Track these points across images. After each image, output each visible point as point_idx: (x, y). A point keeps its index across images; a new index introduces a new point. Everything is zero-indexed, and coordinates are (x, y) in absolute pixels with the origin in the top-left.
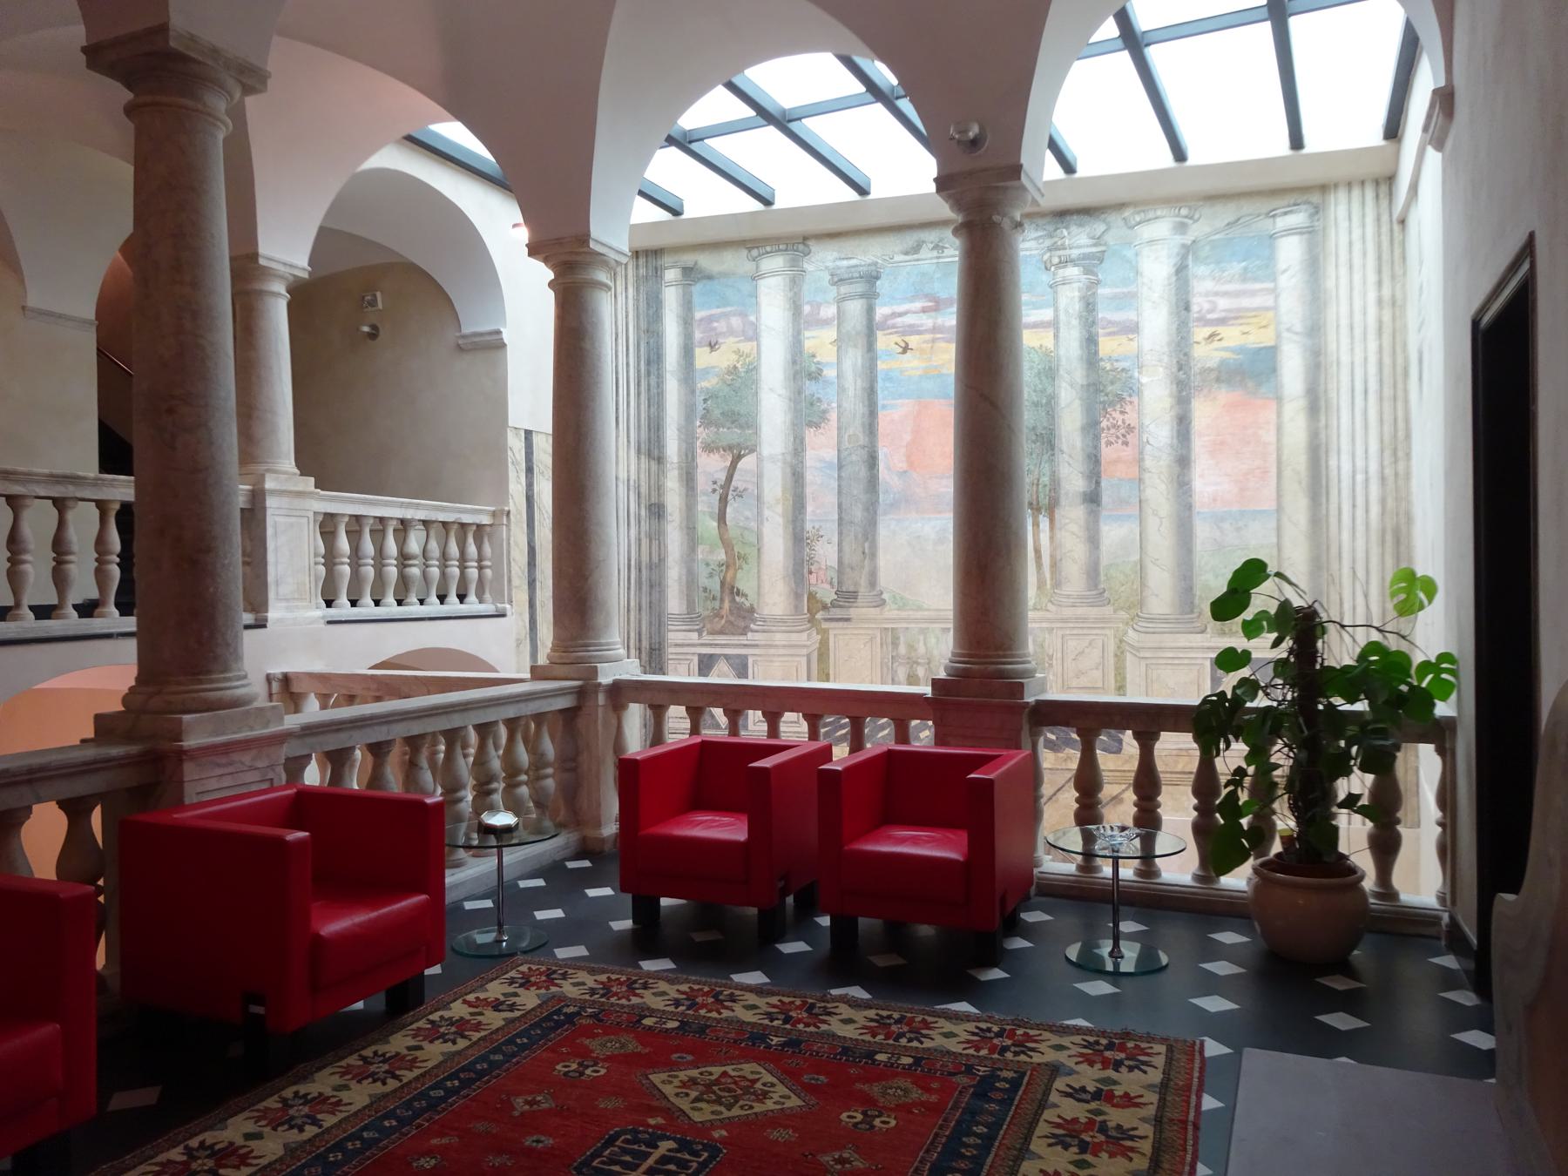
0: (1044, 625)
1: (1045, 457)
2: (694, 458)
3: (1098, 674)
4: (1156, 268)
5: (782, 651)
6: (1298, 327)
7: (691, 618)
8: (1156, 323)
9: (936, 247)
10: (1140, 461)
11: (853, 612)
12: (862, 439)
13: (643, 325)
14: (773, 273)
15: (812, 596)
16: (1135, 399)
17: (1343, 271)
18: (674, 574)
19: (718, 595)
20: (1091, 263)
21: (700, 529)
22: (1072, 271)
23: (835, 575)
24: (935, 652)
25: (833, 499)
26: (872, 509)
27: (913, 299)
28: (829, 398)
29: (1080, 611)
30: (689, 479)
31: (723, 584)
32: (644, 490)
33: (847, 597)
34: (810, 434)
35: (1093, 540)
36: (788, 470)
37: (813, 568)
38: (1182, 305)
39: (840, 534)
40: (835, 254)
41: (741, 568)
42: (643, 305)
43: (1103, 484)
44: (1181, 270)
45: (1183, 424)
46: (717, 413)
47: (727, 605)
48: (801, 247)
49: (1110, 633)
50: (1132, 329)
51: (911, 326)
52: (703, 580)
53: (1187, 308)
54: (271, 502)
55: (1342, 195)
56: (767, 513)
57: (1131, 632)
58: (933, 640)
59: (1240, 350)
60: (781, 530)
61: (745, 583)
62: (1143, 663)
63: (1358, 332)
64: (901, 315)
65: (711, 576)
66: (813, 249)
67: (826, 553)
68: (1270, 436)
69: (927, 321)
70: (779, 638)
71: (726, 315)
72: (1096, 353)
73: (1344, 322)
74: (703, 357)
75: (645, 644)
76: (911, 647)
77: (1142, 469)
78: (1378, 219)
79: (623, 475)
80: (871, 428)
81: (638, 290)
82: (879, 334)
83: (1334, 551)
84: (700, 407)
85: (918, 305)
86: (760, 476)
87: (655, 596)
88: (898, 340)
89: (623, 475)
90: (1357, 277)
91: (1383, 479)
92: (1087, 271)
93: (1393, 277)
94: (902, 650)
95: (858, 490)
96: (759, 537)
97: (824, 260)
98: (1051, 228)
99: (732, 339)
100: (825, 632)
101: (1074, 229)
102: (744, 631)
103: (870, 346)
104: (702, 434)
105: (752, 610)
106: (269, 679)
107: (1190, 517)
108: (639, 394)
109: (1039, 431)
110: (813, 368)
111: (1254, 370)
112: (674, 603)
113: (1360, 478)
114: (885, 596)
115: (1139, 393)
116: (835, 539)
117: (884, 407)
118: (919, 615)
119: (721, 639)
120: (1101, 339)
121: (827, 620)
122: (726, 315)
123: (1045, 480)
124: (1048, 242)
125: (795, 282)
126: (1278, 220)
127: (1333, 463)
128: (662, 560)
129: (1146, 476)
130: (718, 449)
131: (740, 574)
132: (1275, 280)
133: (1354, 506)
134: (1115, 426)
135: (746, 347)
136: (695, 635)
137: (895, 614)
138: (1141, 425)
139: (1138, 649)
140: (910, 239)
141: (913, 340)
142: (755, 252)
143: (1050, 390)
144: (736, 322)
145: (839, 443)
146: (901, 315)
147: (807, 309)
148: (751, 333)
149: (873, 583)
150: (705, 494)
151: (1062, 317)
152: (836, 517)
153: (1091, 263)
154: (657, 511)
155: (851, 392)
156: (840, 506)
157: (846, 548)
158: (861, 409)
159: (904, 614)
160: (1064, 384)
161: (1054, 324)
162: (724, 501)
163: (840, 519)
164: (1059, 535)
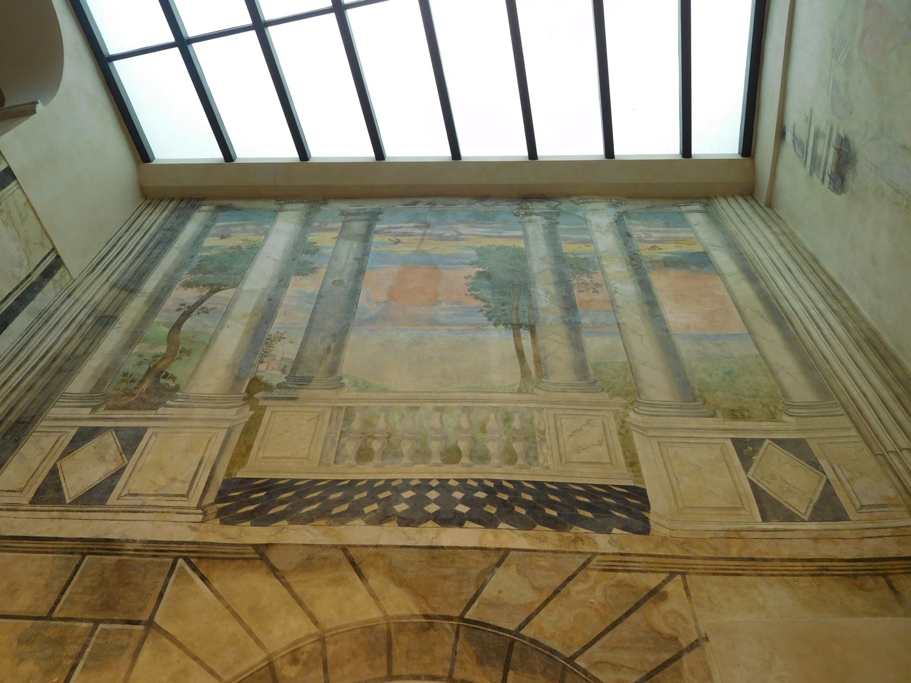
3: (602, 450)
11: (302, 393)
29: (571, 396)
57: (632, 414)
58: (397, 417)
60: (240, 334)
62: (654, 442)
65: (140, 364)
76: (367, 423)
83: (817, 355)
90: (751, 226)
94: (356, 425)
102: (155, 407)
107: (669, 336)
114: (345, 381)
117: (371, 268)
118: (382, 396)
127: (785, 304)
133: (819, 328)
137: (354, 394)
139: (645, 429)
164: (540, 342)
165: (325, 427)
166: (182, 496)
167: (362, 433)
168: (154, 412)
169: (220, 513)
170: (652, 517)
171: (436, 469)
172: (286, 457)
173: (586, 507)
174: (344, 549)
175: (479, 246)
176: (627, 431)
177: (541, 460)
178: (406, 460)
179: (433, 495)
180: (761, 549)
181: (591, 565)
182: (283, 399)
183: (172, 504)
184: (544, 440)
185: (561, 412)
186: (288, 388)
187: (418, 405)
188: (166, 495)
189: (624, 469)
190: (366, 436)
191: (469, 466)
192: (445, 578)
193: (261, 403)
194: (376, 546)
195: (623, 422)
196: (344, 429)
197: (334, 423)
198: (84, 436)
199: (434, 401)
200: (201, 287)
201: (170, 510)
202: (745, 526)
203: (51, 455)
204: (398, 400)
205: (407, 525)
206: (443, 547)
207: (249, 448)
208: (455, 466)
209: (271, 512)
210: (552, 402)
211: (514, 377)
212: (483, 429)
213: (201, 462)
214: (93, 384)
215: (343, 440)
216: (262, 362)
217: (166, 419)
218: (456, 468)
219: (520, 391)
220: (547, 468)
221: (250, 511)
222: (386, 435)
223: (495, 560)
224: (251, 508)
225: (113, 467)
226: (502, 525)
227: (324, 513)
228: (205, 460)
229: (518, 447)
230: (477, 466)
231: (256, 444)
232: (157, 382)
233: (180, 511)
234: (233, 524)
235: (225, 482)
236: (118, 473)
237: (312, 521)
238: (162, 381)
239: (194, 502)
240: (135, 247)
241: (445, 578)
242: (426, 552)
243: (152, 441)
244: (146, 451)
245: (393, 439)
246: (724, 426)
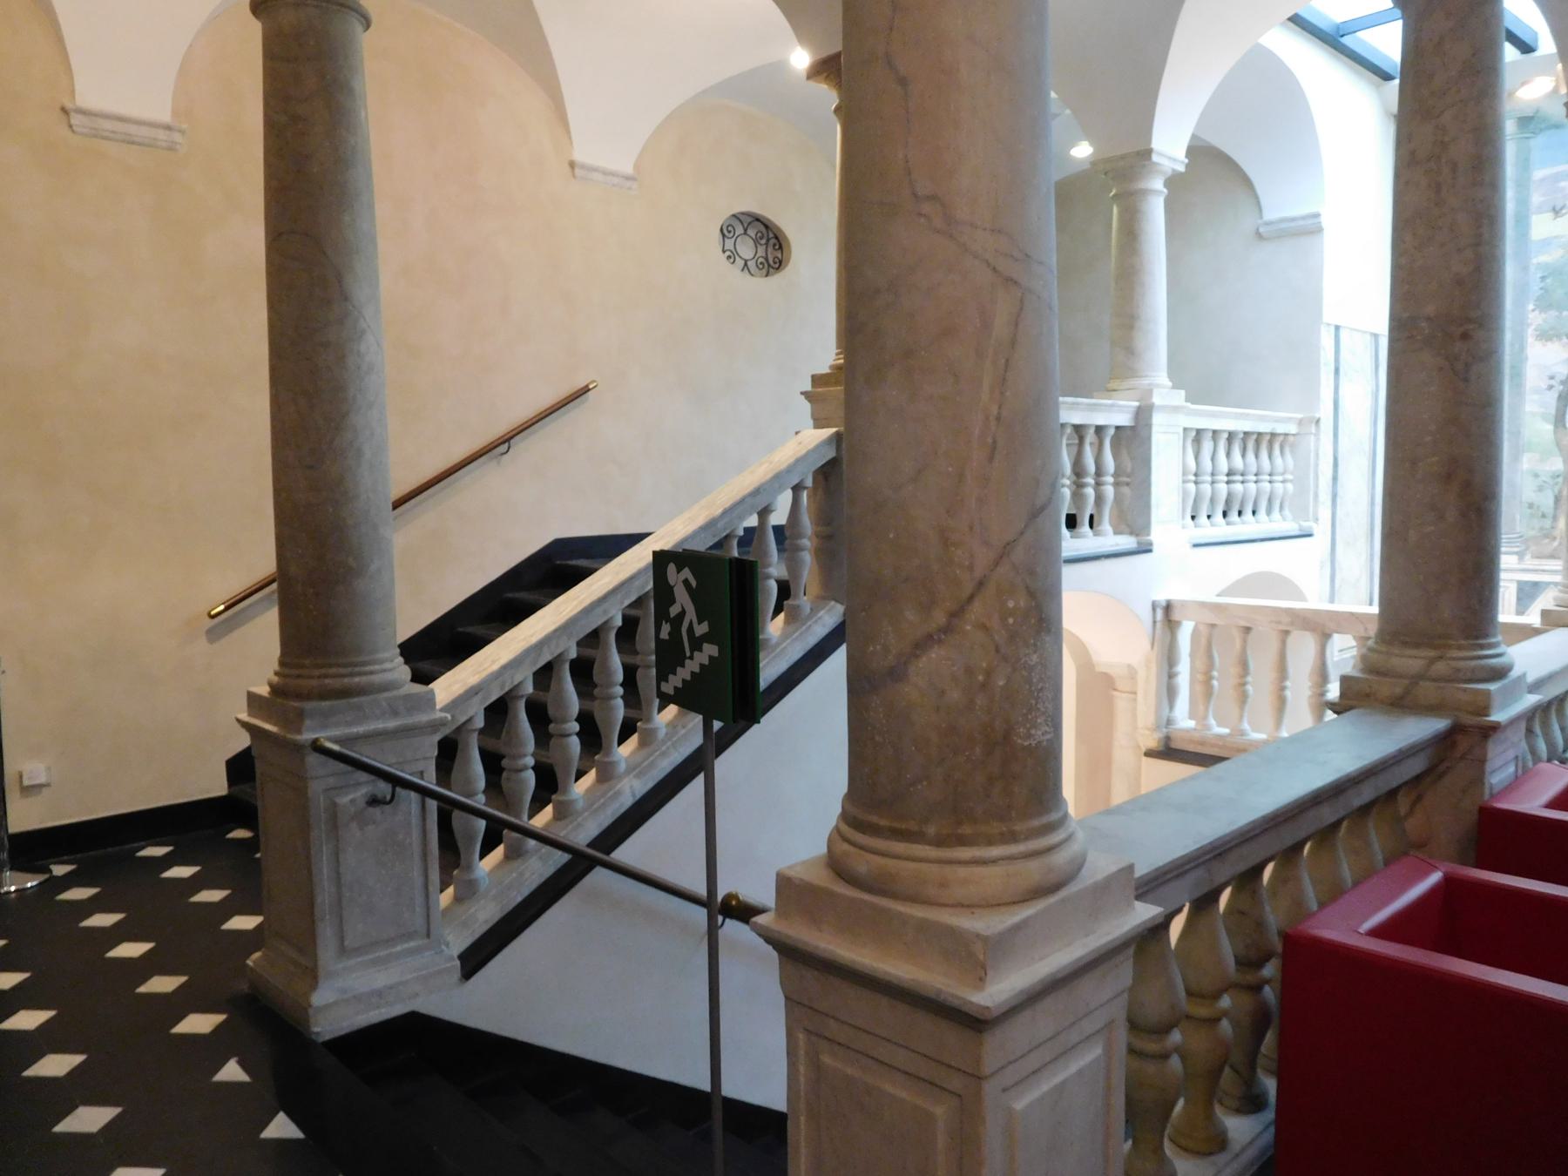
54: (1158, 420)
65: (1540, 489)
106: (1154, 606)
130: (1559, 337)
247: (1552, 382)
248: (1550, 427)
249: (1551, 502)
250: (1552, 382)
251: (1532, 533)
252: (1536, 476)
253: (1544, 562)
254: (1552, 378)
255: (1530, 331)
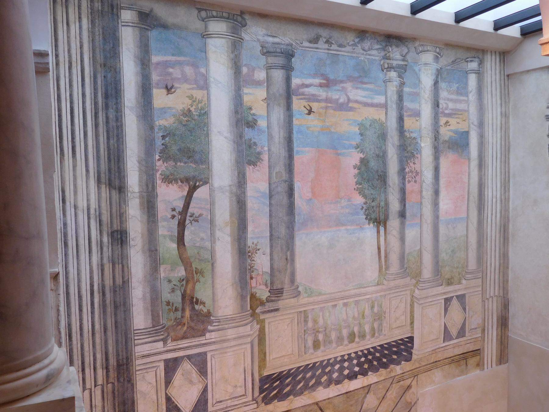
0: (382, 293)
1: (382, 190)
2: (154, 188)
3: (403, 317)
4: (427, 80)
5: (233, 343)
6: (476, 123)
7: (157, 330)
8: (426, 111)
9: (327, 42)
10: (421, 192)
11: (281, 304)
12: (285, 176)
13: (100, 58)
14: (219, 35)
15: (253, 296)
16: (419, 156)
17: (490, 96)
18: (138, 293)
19: (180, 306)
20: (402, 70)
21: (161, 250)
22: (393, 74)
23: (268, 278)
24: (329, 322)
25: (265, 221)
26: (291, 227)
27: (315, 76)
28: (262, 142)
30: (150, 206)
31: (183, 296)
32: (105, 218)
33: (277, 293)
34: (249, 170)
35: (402, 239)
36: (234, 199)
37: (254, 274)
38: (436, 105)
39: (271, 246)
40: (264, 31)
41: (198, 281)
42: (99, 39)
43: (407, 206)
44: (436, 83)
45: (437, 169)
46: (175, 148)
47: (188, 313)
48: (239, 19)
49: (408, 292)
50: (417, 114)
51: (313, 95)
52: (166, 295)
53: (438, 106)
55: (489, 56)
56: (218, 234)
57: (416, 291)
58: (328, 314)
59: (456, 132)
60: (229, 247)
61: (202, 292)
63: (494, 127)
64: (307, 86)
65: (173, 291)
66: (248, 22)
67: (262, 262)
68: (466, 180)
69: (322, 93)
70: (231, 333)
71: (180, 63)
72: (403, 127)
73: (490, 122)
74: (160, 98)
75: (113, 361)
76: (315, 322)
77: (422, 197)
78: (500, 73)
79: (82, 204)
80: (290, 168)
81: (93, 22)
82: (294, 98)
84: (159, 142)
85: (317, 81)
86: (212, 203)
87: (120, 315)
88: (306, 104)
89: (82, 204)
90: (494, 100)
91: (501, 201)
92: (400, 76)
93: (505, 102)
94: (310, 324)
95: (282, 213)
96: (213, 253)
97: (256, 33)
98: (384, 44)
99: (186, 86)
100: (263, 321)
101: (395, 49)
103: (289, 107)
104: (161, 167)
105: (209, 314)
108: (96, 125)
109: (380, 173)
110: (250, 119)
111: (459, 143)
112: (140, 319)
113: (494, 200)
115: (420, 153)
116: (268, 251)
117: (298, 152)
119: (184, 343)
120: (405, 118)
121: (264, 312)
122: (180, 63)
123: (382, 204)
124: (383, 53)
125: (236, 45)
126: (469, 64)
127: (486, 193)
128: (126, 282)
129: (423, 200)
130: (176, 180)
131: (198, 286)
132: (468, 96)
134: (411, 171)
135: (199, 94)
136: (161, 343)
138: (421, 171)
140: (313, 31)
141: (315, 106)
142: (203, 14)
143: (383, 148)
144: (189, 70)
145: (270, 178)
146: (307, 86)
147: (245, 70)
148: (202, 83)
149: (292, 281)
150: (165, 220)
151: (389, 102)
152: (268, 234)
153: (402, 70)
154: (120, 237)
155: (277, 140)
156: (271, 225)
157: (276, 257)
158: (283, 153)
159: (311, 300)
160: (390, 145)
161: (385, 106)
162: (182, 226)
163: (271, 235)
165: (296, 328)
166: (243, 395)
167: (314, 330)
168: (203, 338)
169: (264, 399)
170: (414, 351)
171: (346, 348)
172: (283, 356)
173: (396, 353)
174: (317, 404)
175: (360, 119)
176: (413, 303)
177: (383, 331)
178: (334, 345)
179: (346, 364)
180: (440, 356)
181: (394, 382)
182: (272, 311)
183: (241, 402)
184: (385, 317)
185: (392, 296)
186: (272, 301)
187: (335, 303)
188: (236, 398)
189: (409, 327)
190: (316, 332)
191: (358, 343)
192: (352, 406)
193: (262, 317)
194: (328, 399)
195: (413, 296)
196: (305, 329)
197: (300, 325)
198: (171, 367)
199: (343, 298)
200: (180, 183)
201: (241, 405)
202: (437, 347)
203: (159, 387)
204: (327, 301)
205: (338, 384)
206: (350, 391)
207: (265, 354)
208: (353, 344)
209: (284, 392)
210: (390, 289)
211: (376, 274)
212: (363, 316)
213: (245, 371)
214: (150, 317)
215: (306, 336)
216: (252, 278)
217: (214, 343)
218: (354, 345)
219: (378, 284)
220: (385, 335)
221: (276, 394)
222: (324, 329)
223: (367, 391)
224: (275, 392)
225: (200, 387)
226: (370, 373)
227: (306, 387)
228: (246, 369)
229: (376, 325)
230: (361, 342)
231: (267, 351)
232: (193, 308)
233: (245, 404)
234: (270, 403)
235: (261, 380)
236: (205, 390)
237: (303, 393)
238: (197, 307)
239: (250, 398)
240: (84, 103)
241: (352, 406)
242: (345, 395)
243: (213, 362)
244: (214, 371)
245: (327, 330)
246: (445, 291)
247: (174, 213)
248: (175, 246)
249: (180, 299)
250: (174, 213)
251: (169, 323)
252: (170, 281)
253: (179, 342)
254: (174, 210)
255: (158, 175)
